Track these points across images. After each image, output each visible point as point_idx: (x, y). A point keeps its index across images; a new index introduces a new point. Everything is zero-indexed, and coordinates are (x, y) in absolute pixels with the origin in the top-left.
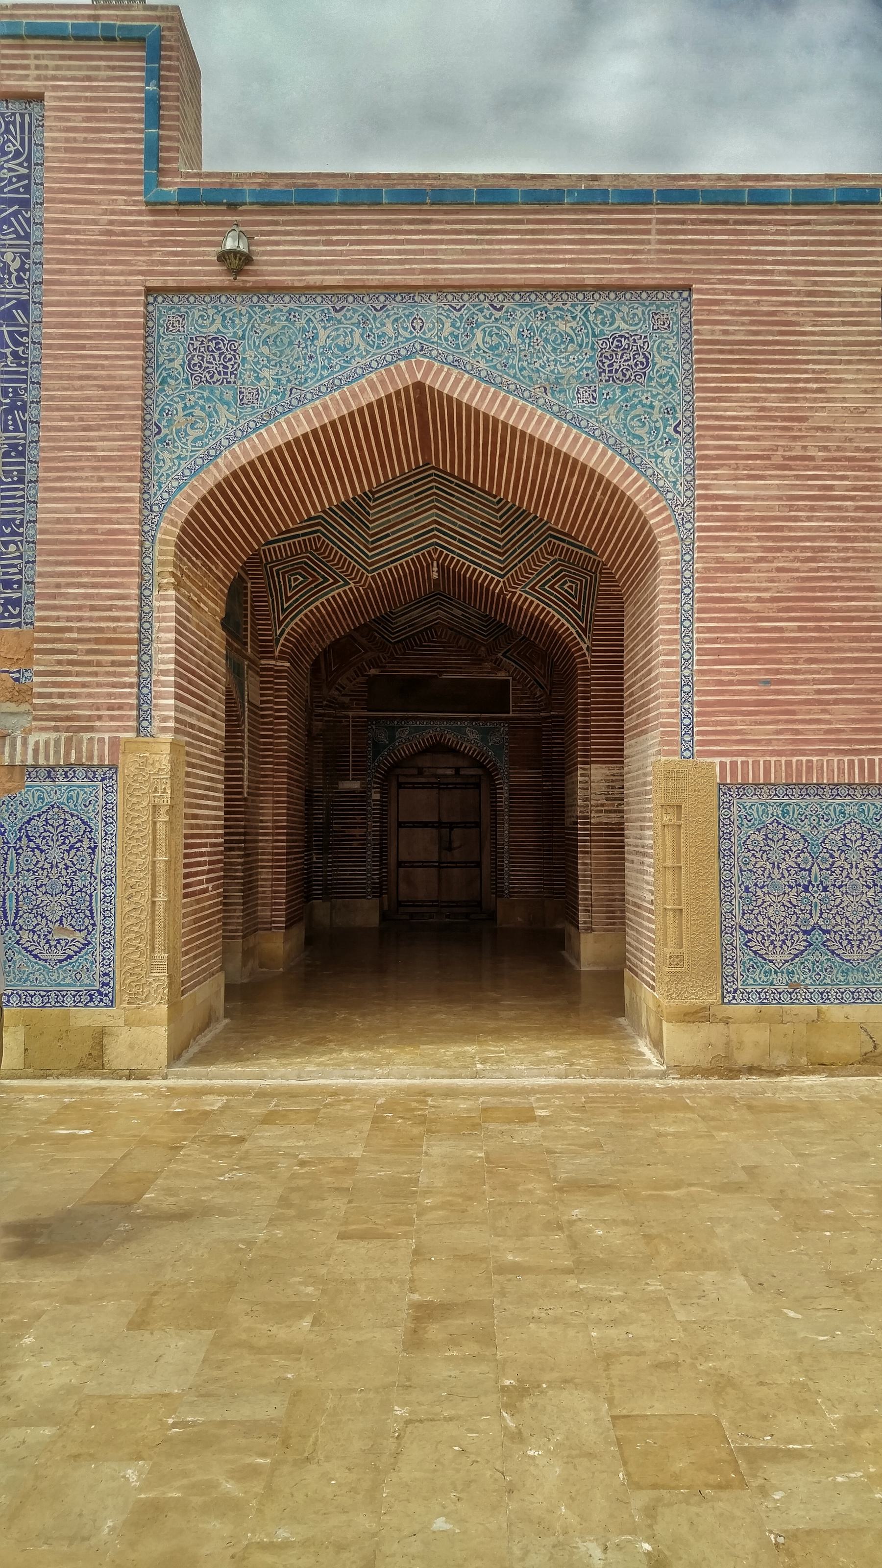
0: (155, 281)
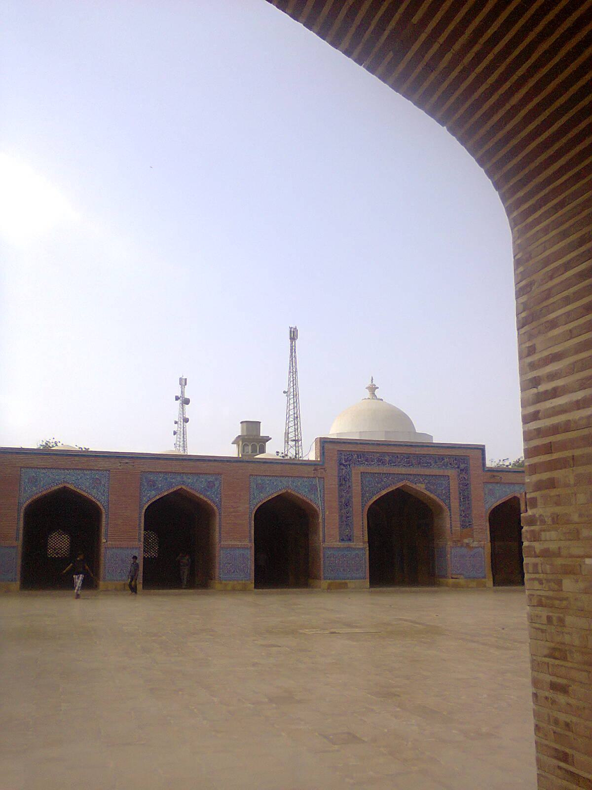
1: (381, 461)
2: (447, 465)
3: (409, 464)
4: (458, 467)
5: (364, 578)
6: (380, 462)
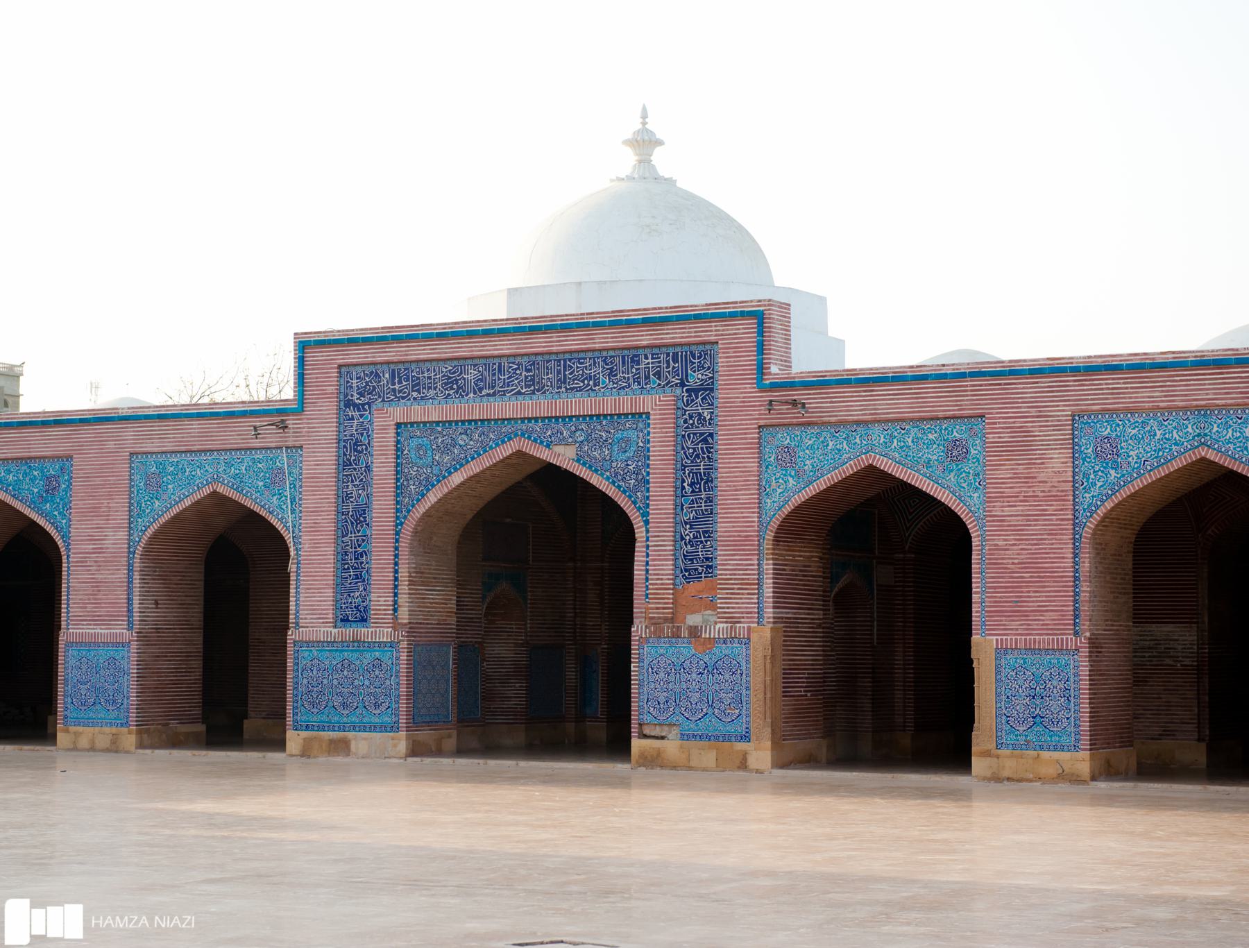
0: (762, 422)
1: (454, 386)
2: (647, 377)
3: (535, 387)
4: (682, 385)
5: (394, 728)
6: (452, 388)
